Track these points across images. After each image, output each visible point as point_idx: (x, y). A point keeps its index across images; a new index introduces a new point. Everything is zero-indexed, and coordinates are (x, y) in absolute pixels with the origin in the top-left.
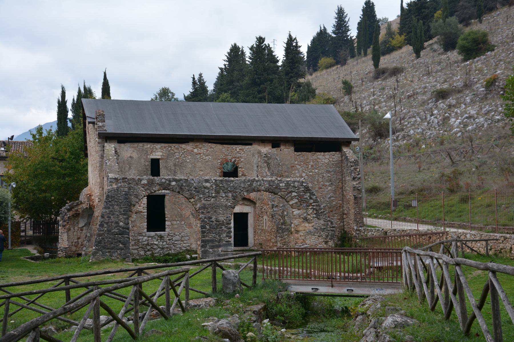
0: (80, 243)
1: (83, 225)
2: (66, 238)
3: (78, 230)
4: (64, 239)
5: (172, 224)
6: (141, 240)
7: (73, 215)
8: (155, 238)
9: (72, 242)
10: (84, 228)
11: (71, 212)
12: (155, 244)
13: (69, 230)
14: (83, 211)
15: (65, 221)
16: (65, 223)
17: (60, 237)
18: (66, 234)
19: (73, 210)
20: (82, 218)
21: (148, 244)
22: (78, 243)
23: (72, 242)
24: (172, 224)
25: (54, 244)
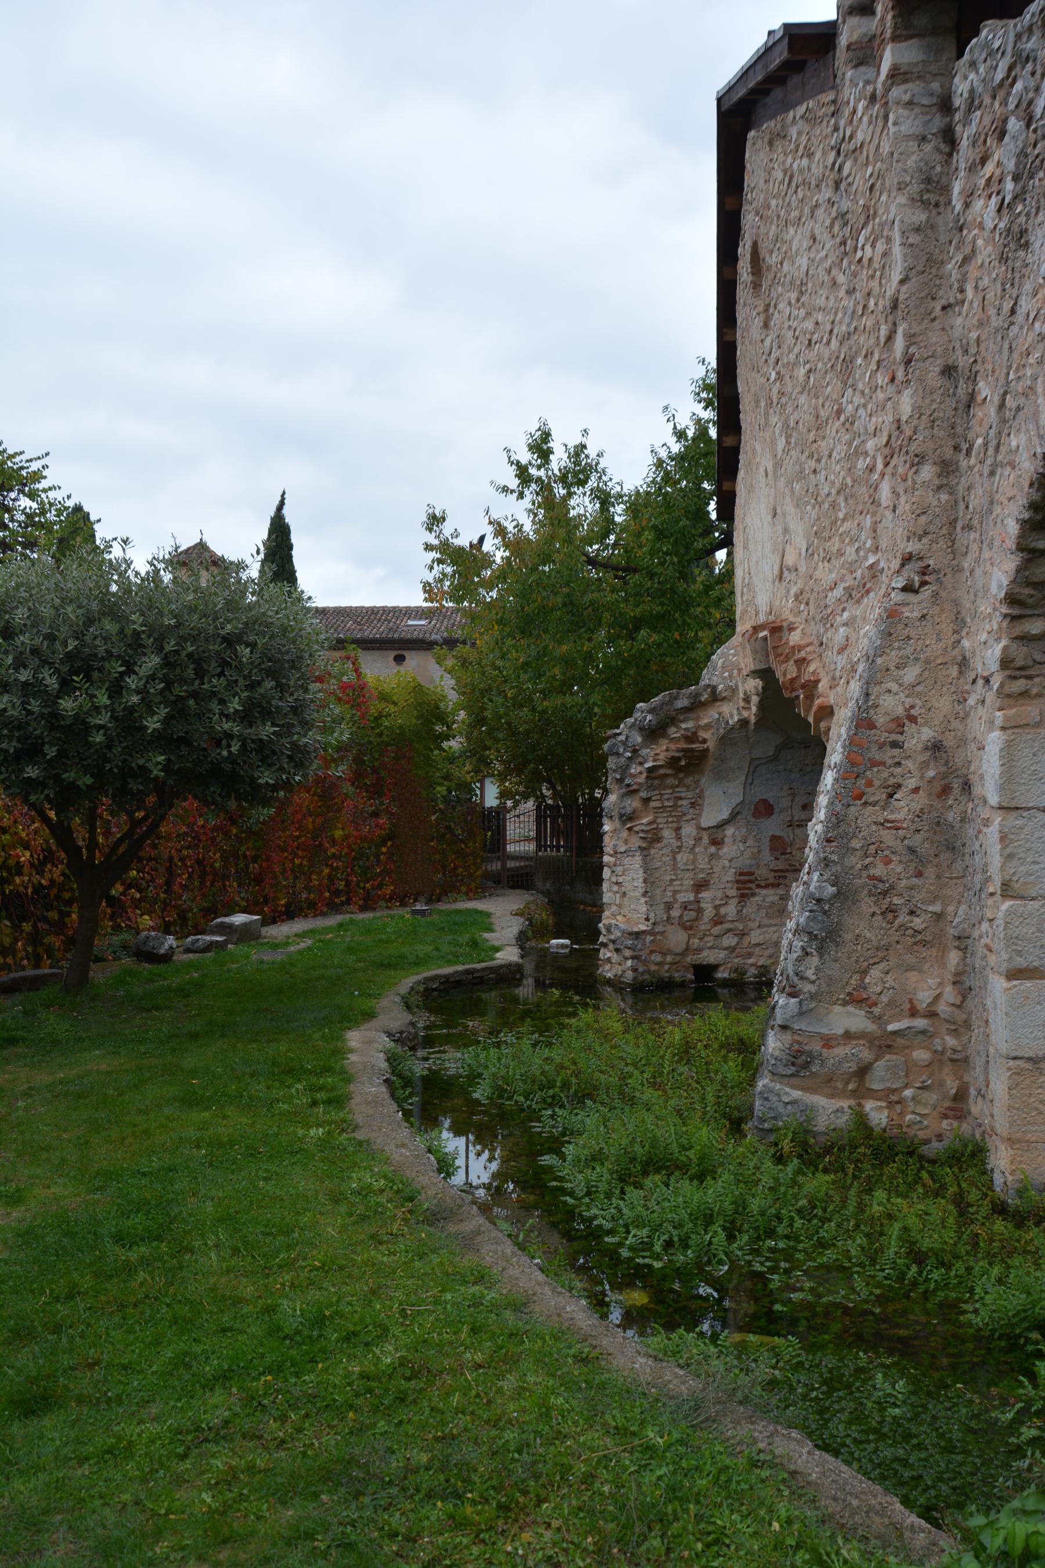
0: (709, 912)
1: (725, 815)
2: (639, 883)
4: (627, 887)
7: (673, 762)
9: (669, 907)
10: (730, 831)
11: (664, 744)
13: (653, 838)
14: (723, 740)
16: (633, 804)
17: (606, 873)
18: (638, 859)
20: (719, 776)
22: (700, 911)
23: (669, 907)
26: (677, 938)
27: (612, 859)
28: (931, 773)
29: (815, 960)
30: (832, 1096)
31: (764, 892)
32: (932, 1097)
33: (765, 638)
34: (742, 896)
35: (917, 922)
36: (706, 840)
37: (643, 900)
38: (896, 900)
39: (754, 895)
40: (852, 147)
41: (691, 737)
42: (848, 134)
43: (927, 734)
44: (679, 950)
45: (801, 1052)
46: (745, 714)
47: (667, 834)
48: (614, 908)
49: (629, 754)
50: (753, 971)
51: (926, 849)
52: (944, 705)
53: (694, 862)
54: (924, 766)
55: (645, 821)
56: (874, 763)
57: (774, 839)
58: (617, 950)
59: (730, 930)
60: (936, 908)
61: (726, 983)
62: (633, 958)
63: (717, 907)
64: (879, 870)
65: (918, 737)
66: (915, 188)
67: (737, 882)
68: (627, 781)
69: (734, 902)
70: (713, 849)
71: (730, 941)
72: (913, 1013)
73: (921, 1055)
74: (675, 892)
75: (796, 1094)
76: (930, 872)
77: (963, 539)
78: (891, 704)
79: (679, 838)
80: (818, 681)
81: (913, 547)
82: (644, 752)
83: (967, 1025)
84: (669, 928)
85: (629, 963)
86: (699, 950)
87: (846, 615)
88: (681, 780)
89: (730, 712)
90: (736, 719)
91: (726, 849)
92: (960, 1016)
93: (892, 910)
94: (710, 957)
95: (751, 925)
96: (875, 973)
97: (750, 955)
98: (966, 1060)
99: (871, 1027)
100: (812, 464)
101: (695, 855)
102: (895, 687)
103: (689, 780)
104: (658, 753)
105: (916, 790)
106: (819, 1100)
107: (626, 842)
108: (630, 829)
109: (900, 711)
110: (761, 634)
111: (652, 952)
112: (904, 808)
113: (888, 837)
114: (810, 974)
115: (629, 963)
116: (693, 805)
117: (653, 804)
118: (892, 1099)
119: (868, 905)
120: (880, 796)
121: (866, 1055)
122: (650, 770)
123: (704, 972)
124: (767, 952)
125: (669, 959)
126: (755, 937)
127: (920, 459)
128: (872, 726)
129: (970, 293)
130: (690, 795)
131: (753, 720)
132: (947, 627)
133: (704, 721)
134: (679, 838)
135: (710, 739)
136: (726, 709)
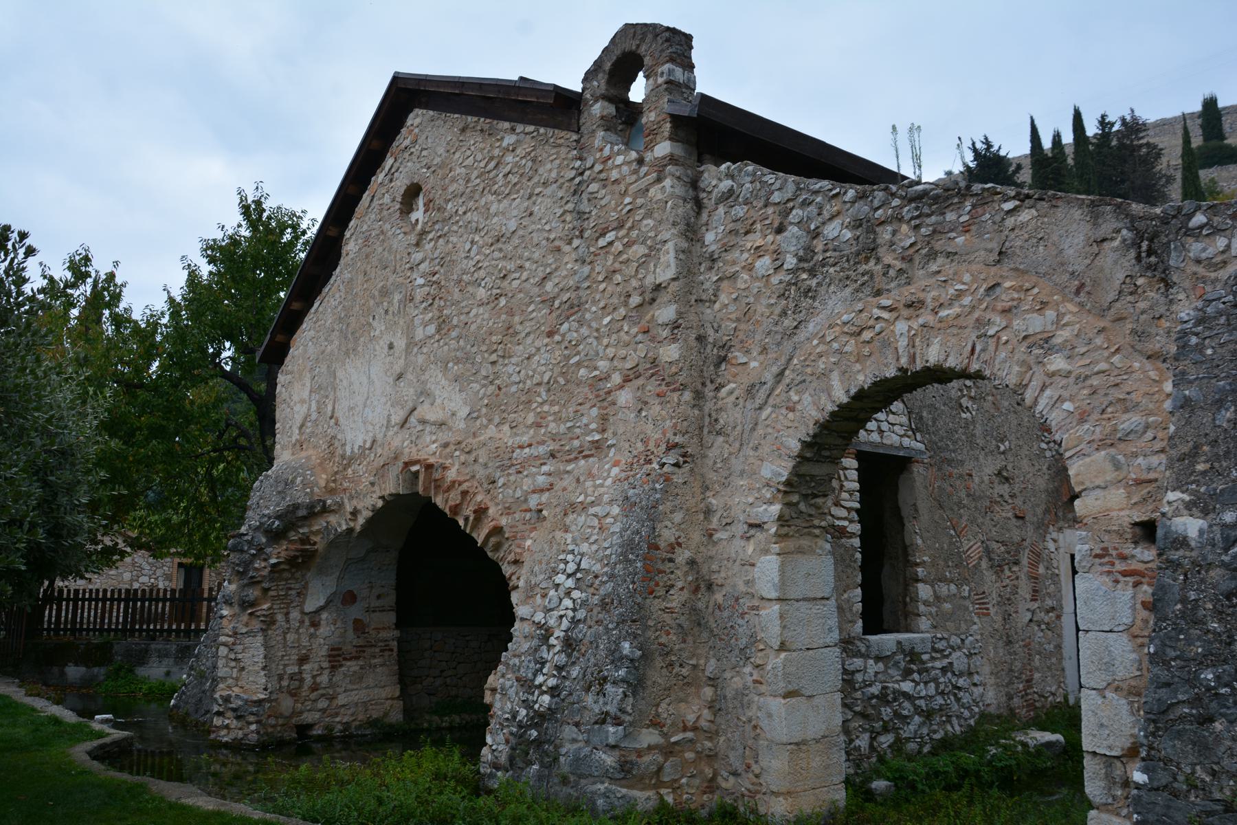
1: (322, 602)
2: (260, 659)
3: (302, 622)
5: (937, 598)
6: (859, 677)
8: (896, 664)
9: (281, 678)
10: (324, 615)
12: (906, 695)
13: (269, 622)
14: (332, 545)
15: (253, 583)
16: (254, 593)
19: (293, 536)
21: (883, 698)
22: (302, 680)
23: (281, 678)
24: (937, 598)
25: (56, 670)
26: (287, 704)
27: (231, 640)
28: (690, 578)
29: (631, 700)
30: (643, 789)
31: (349, 663)
32: (697, 782)
33: (416, 474)
34: (333, 667)
35: (685, 671)
36: (307, 623)
37: (262, 673)
38: (673, 658)
39: (341, 666)
40: (603, 176)
41: (305, 540)
42: (598, 167)
43: (687, 554)
44: (287, 714)
45: (626, 762)
46: (352, 524)
47: (280, 617)
48: (230, 681)
49: (253, 552)
50: (339, 727)
51: (686, 625)
52: (697, 536)
53: (299, 639)
54: (686, 574)
55: (265, 607)
56: (660, 572)
57: (356, 621)
58: (238, 718)
59: (323, 695)
60: (693, 662)
61: (320, 739)
62: (257, 722)
63: (314, 677)
64: (663, 640)
65: (682, 556)
66: (682, 227)
67: (329, 656)
68: (251, 574)
69: (327, 672)
70: (312, 630)
71: (323, 704)
72: (685, 729)
73: (690, 755)
74: (285, 665)
75: (624, 791)
76: (690, 639)
77: (708, 439)
78: (667, 535)
79: (288, 621)
80: (487, 509)
81: (678, 439)
82: (268, 550)
83: (717, 733)
84: (280, 696)
85: (253, 727)
86: (301, 713)
87: (545, 468)
88: (293, 574)
89: (340, 523)
90: (344, 527)
91: (321, 630)
92: (714, 728)
93: (671, 664)
94: (308, 718)
95: (339, 690)
96: (663, 705)
97: (337, 714)
98: (716, 755)
99: (661, 741)
100: (494, 357)
101: (299, 634)
102: (670, 525)
103: (298, 575)
104: (277, 554)
105: (682, 589)
106: (636, 793)
107: (247, 625)
108: (251, 614)
109: (673, 540)
110: (414, 468)
111: (269, 716)
112: (676, 599)
113: (667, 618)
114: (629, 709)
115: (253, 727)
116: (299, 594)
117: (272, 593)
118: (675, 787)
119: (659, 662)
120: (662, 593)
121: (661, 759)
122: (274, 565)
123: (303, 729)
124: (350, 712)
125: (281, 721)
126: (342, 700)
127: (684, 387)
128: (657, 548)
129: (724, 298)
130: (297, 586)
131: (358, 528)
132: (698, 490)
133: (316, 528)
134: (288, 621)
135: (320, 543)
136: (333, 519)
